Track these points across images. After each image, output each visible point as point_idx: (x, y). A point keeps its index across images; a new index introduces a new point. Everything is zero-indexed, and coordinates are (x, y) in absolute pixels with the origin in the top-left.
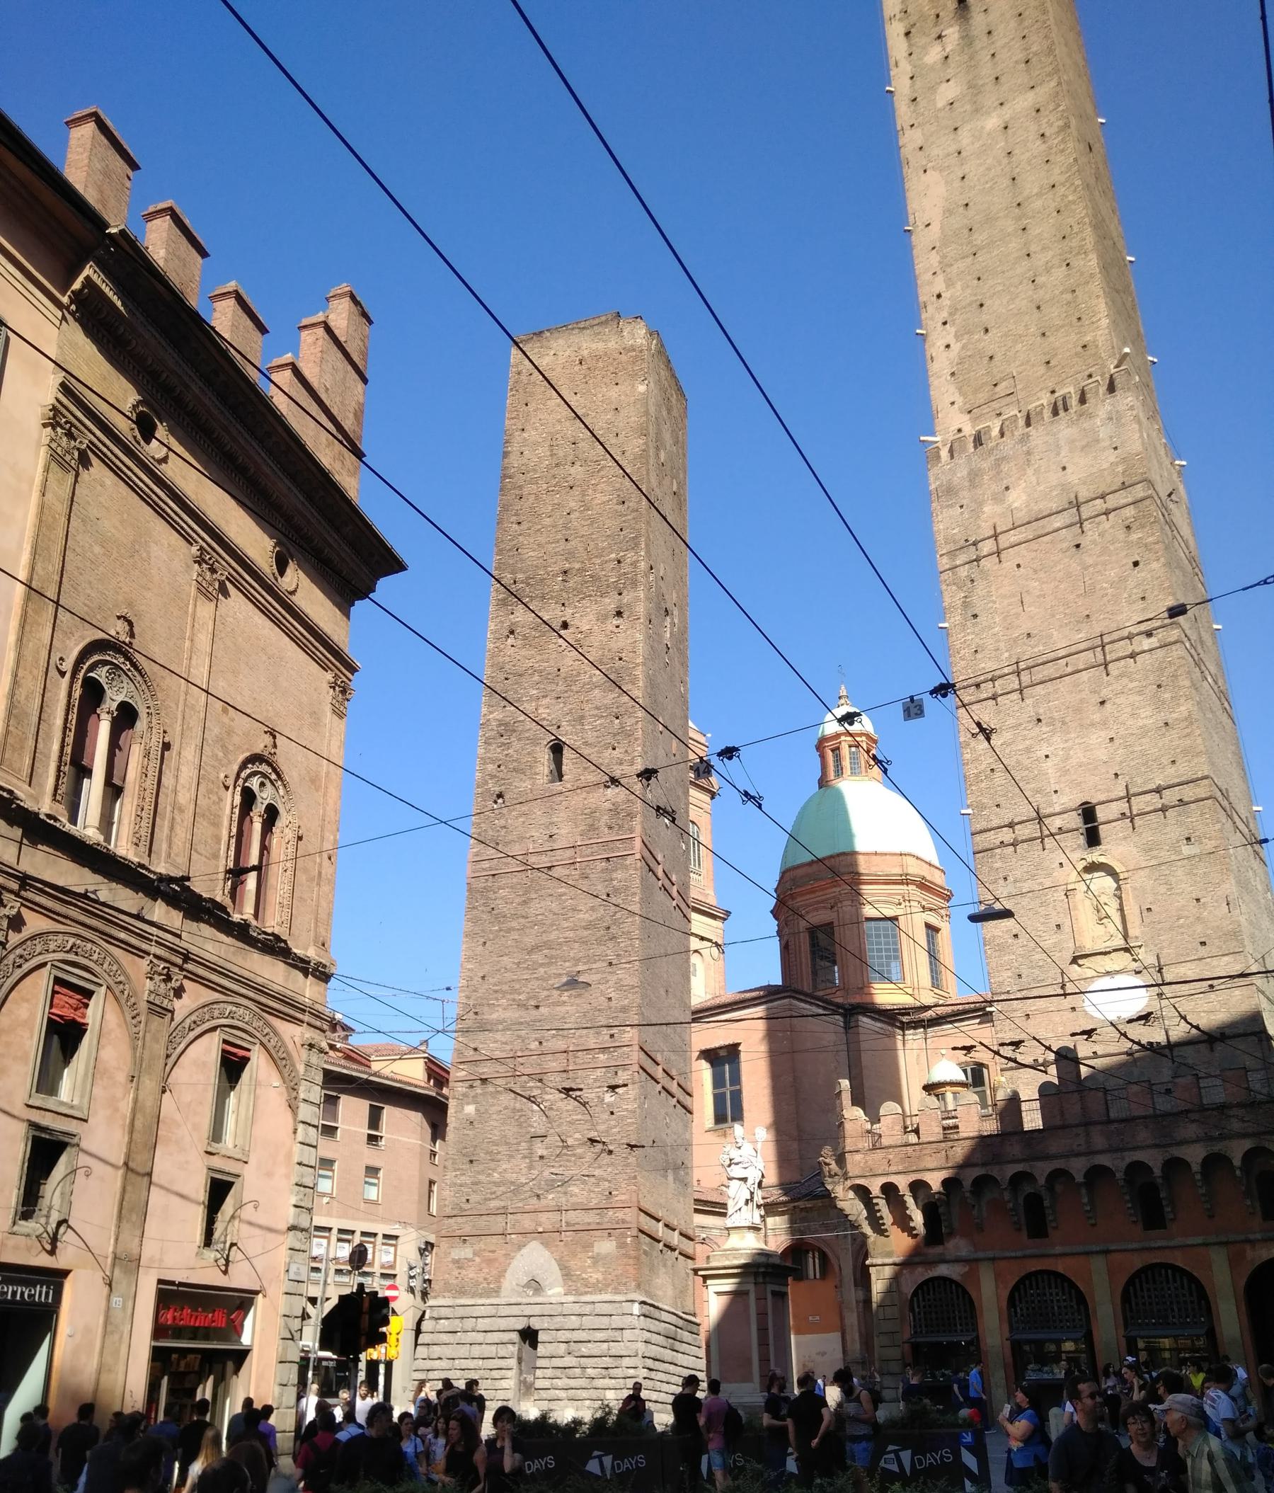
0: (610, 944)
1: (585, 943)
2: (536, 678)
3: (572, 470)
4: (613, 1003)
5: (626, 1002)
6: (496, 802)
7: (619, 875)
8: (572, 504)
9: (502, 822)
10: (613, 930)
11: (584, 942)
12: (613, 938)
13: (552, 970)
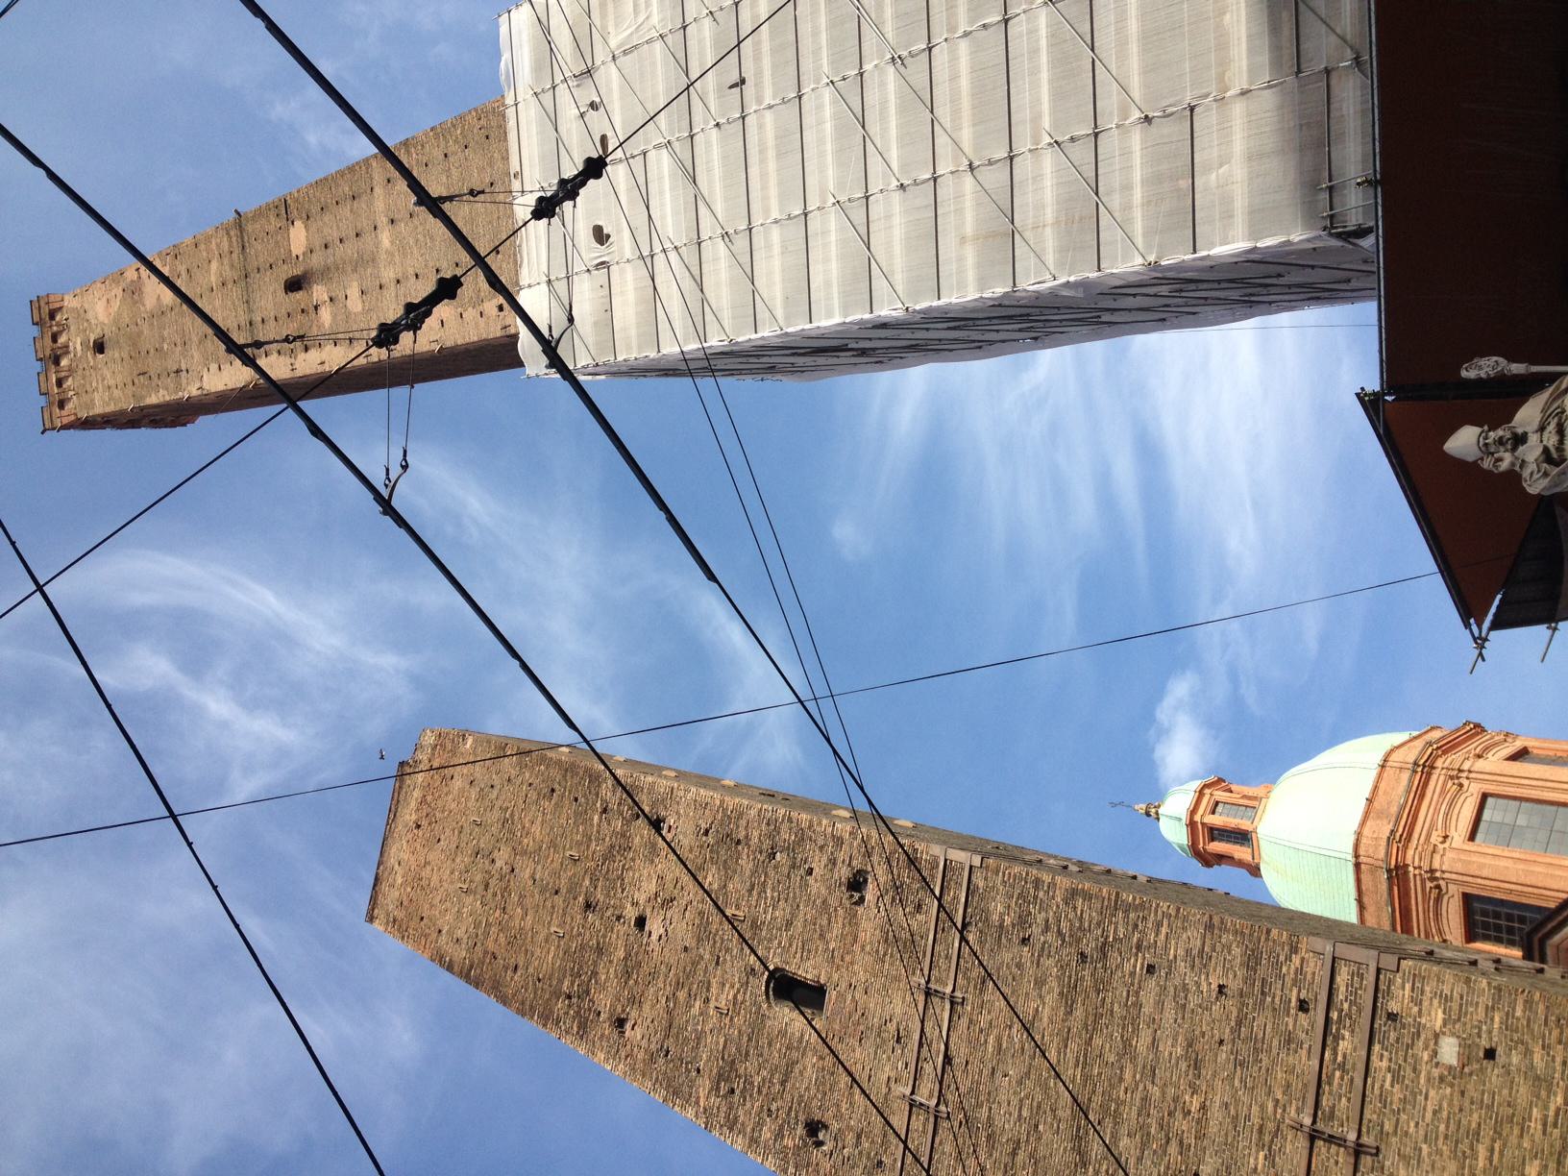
0: (1114, 959)
1: (1098, 1016)
2: (682, 995)
3: (499, 864)
4: (1234, 985)
5: (1236, 951)
6: (819, 1144)
7: (997, 907)
8: (527, 873)
9: (850, 1138)
10: (1089, 946)
11: (1092, 1026)
12: (1103, 949)
13: (1130, 1114)
